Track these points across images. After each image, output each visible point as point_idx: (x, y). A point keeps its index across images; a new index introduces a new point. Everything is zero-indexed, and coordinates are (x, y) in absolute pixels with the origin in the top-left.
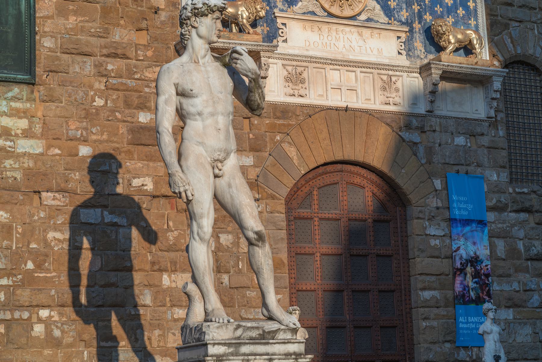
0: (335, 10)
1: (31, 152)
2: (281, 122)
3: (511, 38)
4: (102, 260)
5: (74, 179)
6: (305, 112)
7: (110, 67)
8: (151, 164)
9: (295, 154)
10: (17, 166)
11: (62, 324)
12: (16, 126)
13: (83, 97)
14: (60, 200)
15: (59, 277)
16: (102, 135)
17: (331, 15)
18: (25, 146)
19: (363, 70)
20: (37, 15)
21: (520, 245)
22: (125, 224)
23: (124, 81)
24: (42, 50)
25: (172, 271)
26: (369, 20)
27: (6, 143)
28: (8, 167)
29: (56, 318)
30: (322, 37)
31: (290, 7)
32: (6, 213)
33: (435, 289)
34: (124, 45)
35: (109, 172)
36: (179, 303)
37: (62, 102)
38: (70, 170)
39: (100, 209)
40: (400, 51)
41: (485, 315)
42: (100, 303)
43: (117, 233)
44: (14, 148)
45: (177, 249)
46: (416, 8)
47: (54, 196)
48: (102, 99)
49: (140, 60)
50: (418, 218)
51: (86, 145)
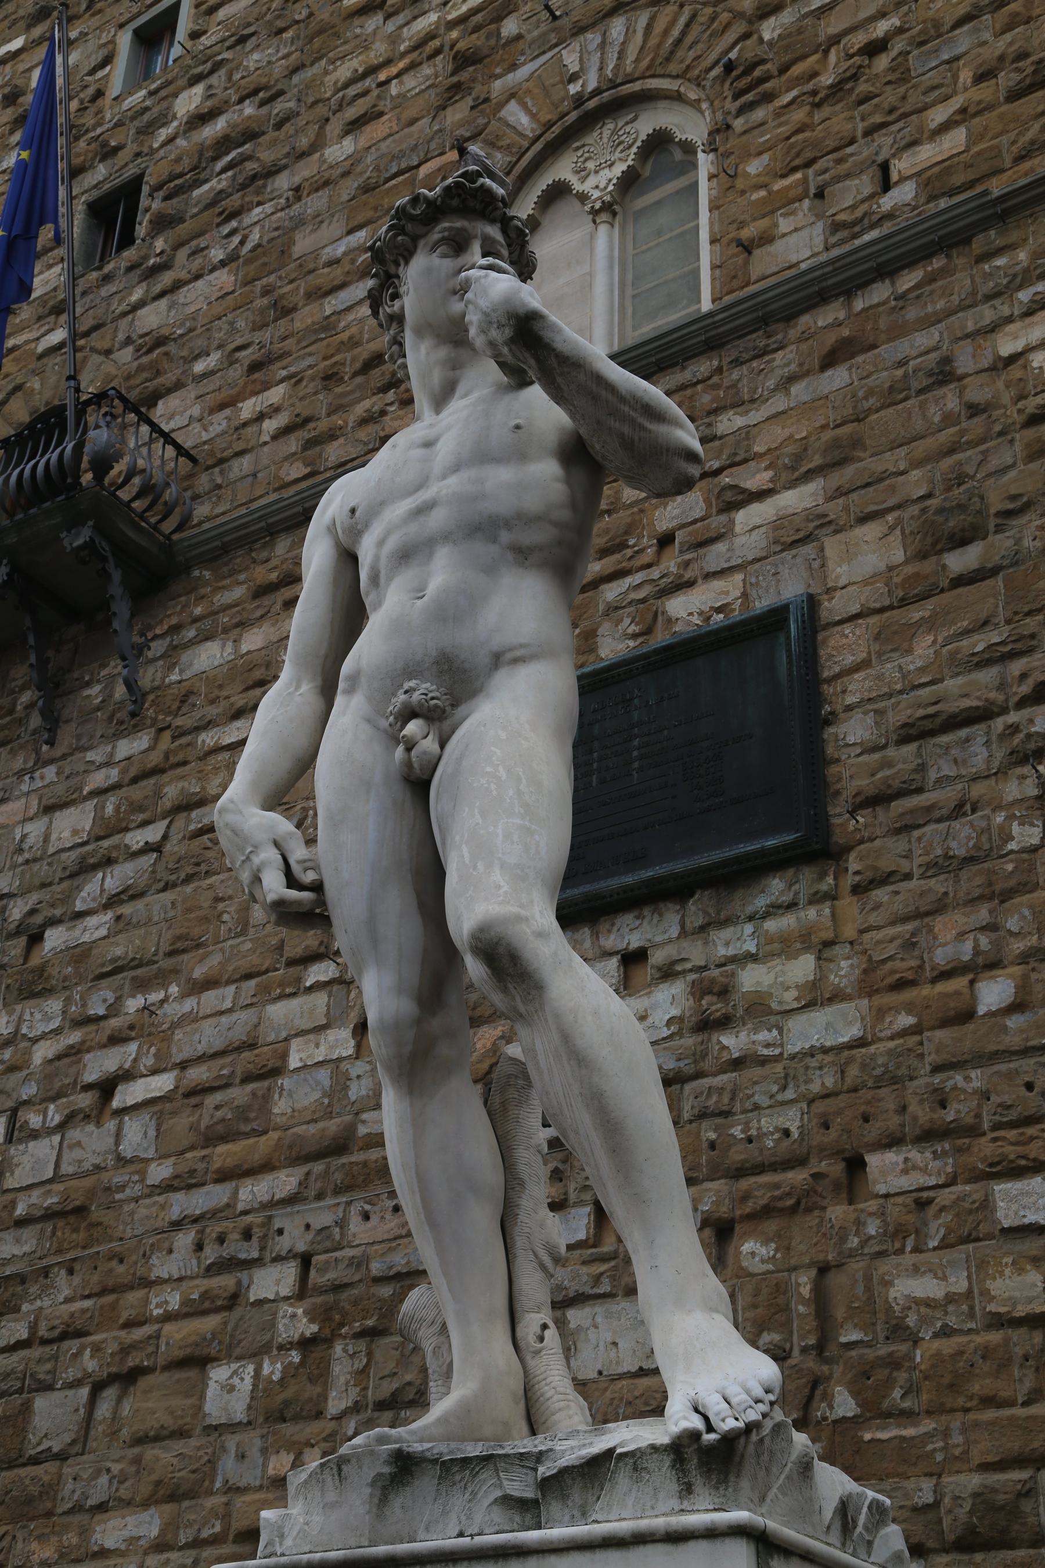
1: (828, 1044)
5: (964, 1091)
10: (790, 1094)
12: (782, 983)
13: (969, 838)
14: (924, 1170)
15: (946, 1434)
18: (812, 1030)
20: (826, 674)
24: (843, 757)
27: (755, 1038)
28: (763, 1100)
32: (765, 1243)
37: (908, 877)
44: (782, 1045)
47: (906, 1160)
48: (1032, 825)
51: (991, 978)
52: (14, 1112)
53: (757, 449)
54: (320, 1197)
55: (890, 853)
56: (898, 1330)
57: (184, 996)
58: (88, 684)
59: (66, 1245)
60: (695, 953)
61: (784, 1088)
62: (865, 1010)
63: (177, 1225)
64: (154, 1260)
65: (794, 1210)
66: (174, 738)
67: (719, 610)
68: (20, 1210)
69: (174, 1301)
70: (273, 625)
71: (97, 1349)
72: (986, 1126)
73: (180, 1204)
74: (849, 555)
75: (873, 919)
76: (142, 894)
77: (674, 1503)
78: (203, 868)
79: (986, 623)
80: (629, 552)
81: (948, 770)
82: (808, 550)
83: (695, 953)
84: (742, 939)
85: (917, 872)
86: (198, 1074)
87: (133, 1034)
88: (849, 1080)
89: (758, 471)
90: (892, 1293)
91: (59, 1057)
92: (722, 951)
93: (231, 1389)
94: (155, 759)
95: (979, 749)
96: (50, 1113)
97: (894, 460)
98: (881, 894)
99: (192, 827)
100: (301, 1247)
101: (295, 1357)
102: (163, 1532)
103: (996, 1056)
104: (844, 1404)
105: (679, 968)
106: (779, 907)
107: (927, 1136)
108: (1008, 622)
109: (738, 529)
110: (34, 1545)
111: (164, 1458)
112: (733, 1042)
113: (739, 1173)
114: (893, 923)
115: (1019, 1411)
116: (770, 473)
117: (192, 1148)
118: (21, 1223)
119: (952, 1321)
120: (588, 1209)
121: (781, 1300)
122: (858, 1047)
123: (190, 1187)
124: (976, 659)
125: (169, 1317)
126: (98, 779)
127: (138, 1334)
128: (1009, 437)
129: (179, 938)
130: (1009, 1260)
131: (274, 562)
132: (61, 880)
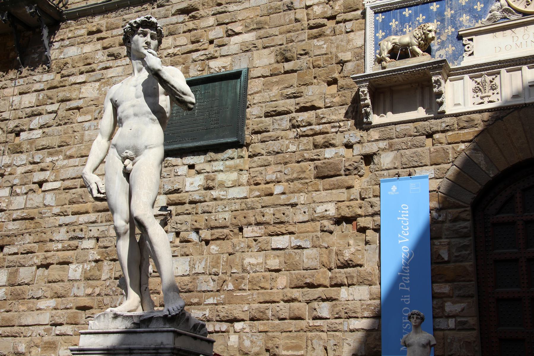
2: (466, 131)
4: (287, 279)
8: (334, 191)
9: (482, 158)
10: (227, 209)
11: (252, 335)
13: (279, 147)
14: (256, 232)
15: (252, 295)
16: (293, 173)
17: (525, 14)
18: (235, 193)
20: (249, 93)
22: (309, 247)
25: (349, 285)
28: (220, 210)
29: (247, 330)
30: (516, 38)
31: (477, 22)
35: (297, 205)
36: (354, 315)
37: (262, 155)
38: (266, 207)
39: (289, 236)
45: (354, 264)
52: (12, 187)
53: (239, 18)
54: (101, 222)
55: (258, 147)
56: (244, 270)
57: (64, 159)
58: (34, 53)
59: (28, 228)
60: (208, 167)
61: (225, 207)
62: (248, 190)
63: (60, 226)
64: (54, 234)
65: (224, 239)
66: (62, 77)
67: (224, 67)
68: (14, 216)
69: (60, 246)
70: (94, 45)
71: (38, 257)
72: (272, 223)
73: (62, 220)
74: (260, 58)
75: (254, 165)
76: (51, 126)
77: (162, 326)
78: (71, 121)
79: (292, 86)
80: (200, 44)
81: (276, 126)
82: (249, 54)
83: (208, 167)
84: (218, 166)
85: (265, 154)
86: (68, 183)
87: (48, 169)
88: (242, 208)
89: (239, 26)
90: (245, 262)
91: (25, 173)
92: (214, 169)
93: (76, 271)
94: (55, 83)
95: (285, 121)
96: (23, 189)
97: (276, 31)
98: (256, 159)
99: (67, 107)
100: (96, 236)
101: (93, 264)
102: (57, 305)
103: (276, 205)
104: (231, 287)
105: (202, 171)
106: (230, 158)
107: (258, 224)
108: (297, 86)
109: (231, 43)
110: (20, 306)
111: (57, 286)
112: (215, 193)
113: (212, 228)
114: (258, 167)
116: (241, 28)
117: (66, 204)
118: (14, 220)
119: (258, 269)
120: (174, 233)
121: (219, 261)
122: (244, 199)
123: (65, 215)
125: (58, 251)
126: (38, 86)
127: (49, 254)
128: (305, 31)
129: (62, 142)
130: (272, 256)
131: (94, 24)
132: (25, 117)
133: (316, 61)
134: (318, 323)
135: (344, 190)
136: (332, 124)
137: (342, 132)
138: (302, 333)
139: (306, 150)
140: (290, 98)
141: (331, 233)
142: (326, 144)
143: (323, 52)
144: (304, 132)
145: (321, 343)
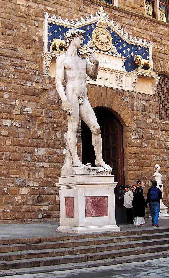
0: (100, 48)
3: (160, 65)
6: (89, 86)
7: (16, 62)
8: (31, 103)
16: (13, 89)
17: (98, 49)
19: (110, 72)
21: (162, 143)
23: (22, 68)
26: (112, 53)
33: (134, 159)
34: (22, 54)
40: (123, 66)
41: (156, 169)
42: (10, 159)
43: (18, 130)
46: (129, 50)
49: (28, 61)
50: (128, 131)
115: (2, 146)
124: (9, 48)
133: (22, 35)
134: (26, 163)
135: (35, 103)
136: (30, 70)
137: (34, 75)
138: (18, 167)
139: (18, 79)
140: (11, 49)
141: (30, 122)
142: (28, 79)
143: (26, 32)
144: (18, 69)
145: (28, 172)
